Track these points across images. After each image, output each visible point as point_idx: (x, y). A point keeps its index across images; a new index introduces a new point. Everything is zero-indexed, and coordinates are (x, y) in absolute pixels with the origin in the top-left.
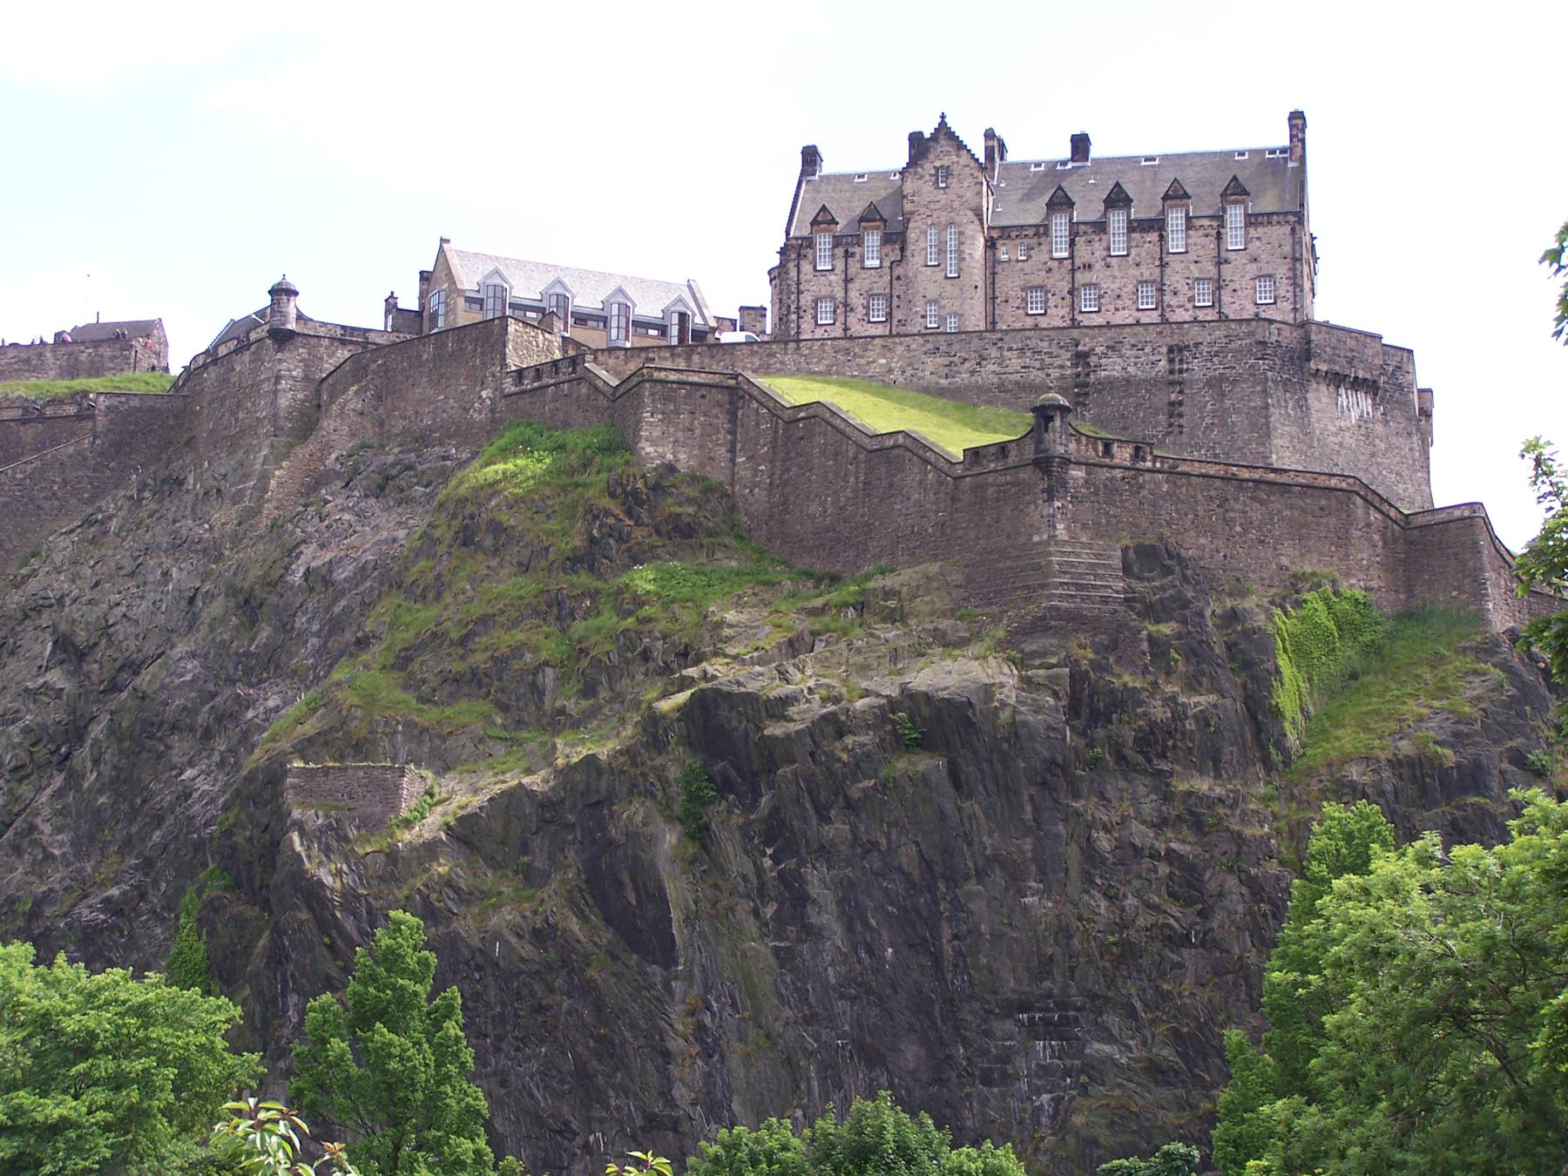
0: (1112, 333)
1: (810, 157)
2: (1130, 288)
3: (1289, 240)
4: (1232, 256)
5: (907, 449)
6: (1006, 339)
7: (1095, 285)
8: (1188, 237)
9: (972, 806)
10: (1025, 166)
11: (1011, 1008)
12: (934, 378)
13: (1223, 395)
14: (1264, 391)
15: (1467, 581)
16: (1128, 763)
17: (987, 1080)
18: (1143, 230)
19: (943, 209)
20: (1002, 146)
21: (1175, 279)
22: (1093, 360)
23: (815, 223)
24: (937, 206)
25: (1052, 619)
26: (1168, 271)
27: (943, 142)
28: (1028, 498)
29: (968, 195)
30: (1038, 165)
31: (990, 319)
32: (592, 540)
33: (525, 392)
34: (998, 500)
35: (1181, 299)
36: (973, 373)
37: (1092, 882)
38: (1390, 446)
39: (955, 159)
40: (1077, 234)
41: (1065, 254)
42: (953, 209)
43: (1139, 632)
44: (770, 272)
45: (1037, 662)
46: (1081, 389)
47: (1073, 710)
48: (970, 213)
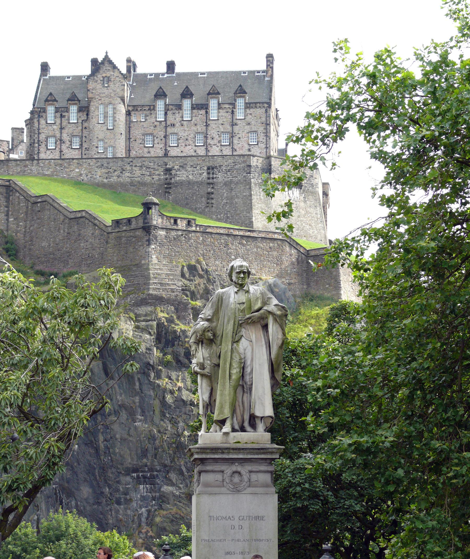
1: (45, 67)
2: (192, 135)
3: (265, 115)
4: (239, 122)
5: (86, 219)
6: (134, 161)
7: (176, 134)
8: (219, 112)
9: (111, 383)
10: (145, 75)
11: (128, 472)
12: (101, 179)
13: (232, 189)
14: (250, 188)
15: (333, 281)
16: (181, 364)
17: (119, 503)
18: (198, 109)
19: (107, 96)
20: (135, 65)
21: (213, 132)
22: (173, 172)
23: (47, 100)
24: (104, 95)
25: (150, 299)
26: (209, 128)
27: (106, 65)
28: (140, 243)
30: (151, 75)
31: (128, 148)
34: (126, 244)
35: (215, 141)
36: (119, 177)
37: (164, 416)
38: (307, 212)
39: (112, 73)
40: (168, 110)
42: (111, 97)
43: (187, 305)
44: (26, 121)
45: (142, 318)
46: (167, 187)
47: (158, 339)
48: (119, 99)
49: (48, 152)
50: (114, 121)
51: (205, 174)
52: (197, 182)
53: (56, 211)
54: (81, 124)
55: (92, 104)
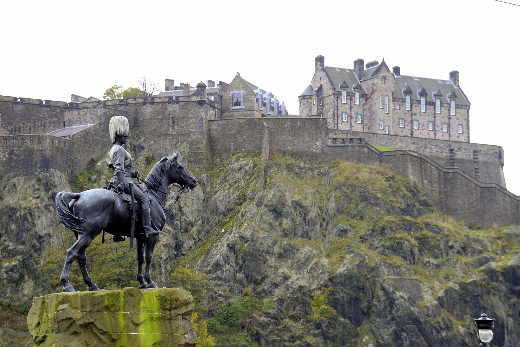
0: (459, 144)
1: (320, 60)
2: (426, 123)
4: (452, 117)
5: (497, 189)
6: (432, 142)
7: (417, 121)
8: (441, 109)
18: (430, 105)
21: (438, 122)
22: (454, 151)
26: (436, 119)
29: (391, 87)
32: (408, 205)
33: (338, 146)
41: (409, 110)
49: (343, 124)
50: (389, 108)
51: (472, 155)
52: (468, 160)
53: (468, 181)
54: (362, 107)
55: (375, 93)
